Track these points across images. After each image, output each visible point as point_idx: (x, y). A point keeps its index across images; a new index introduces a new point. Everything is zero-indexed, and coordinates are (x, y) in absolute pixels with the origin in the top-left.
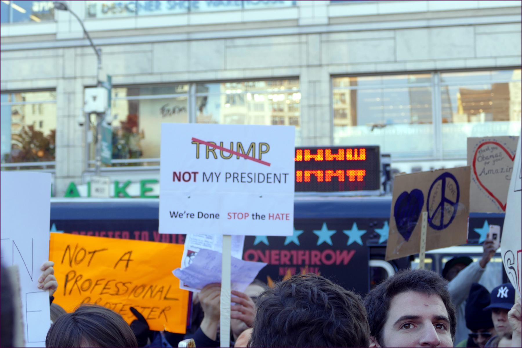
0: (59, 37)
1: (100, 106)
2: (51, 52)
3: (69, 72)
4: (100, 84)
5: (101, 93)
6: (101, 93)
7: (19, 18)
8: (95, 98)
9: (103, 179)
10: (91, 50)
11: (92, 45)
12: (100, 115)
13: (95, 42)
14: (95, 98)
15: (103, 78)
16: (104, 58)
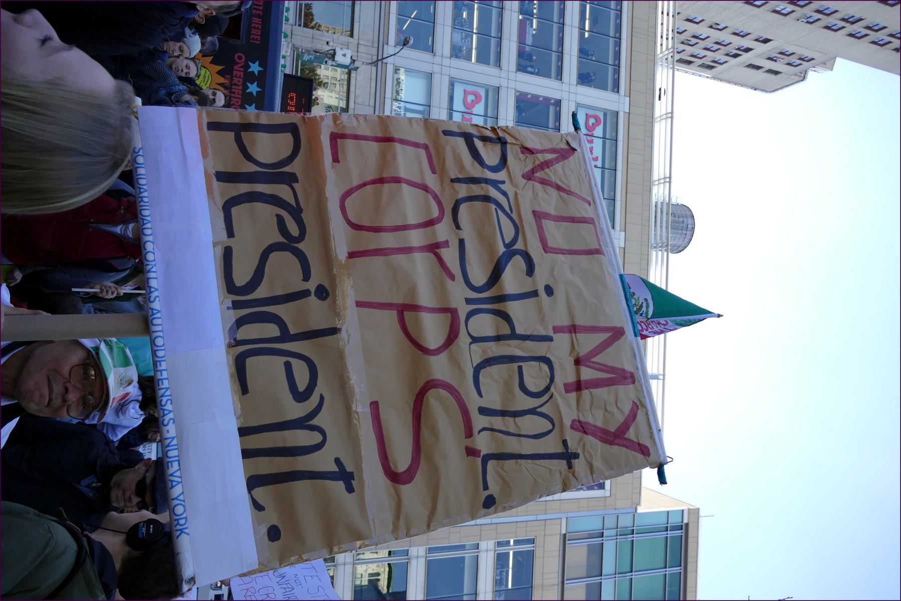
0: (385, 46)
1: (339, 58)
2: (376, 39)
3: (361, 49)
4: (353, 61)
5: (347, 61)
6: (347, 61)
7: (400, 23)
8: (344, 55)
9: (289, 50)
10: (375, 58)
11: (378, 60)
12: (333, 56)
13: (380, 63)
14: (344, 55)
15: (356, 64)
16: (369, 67)
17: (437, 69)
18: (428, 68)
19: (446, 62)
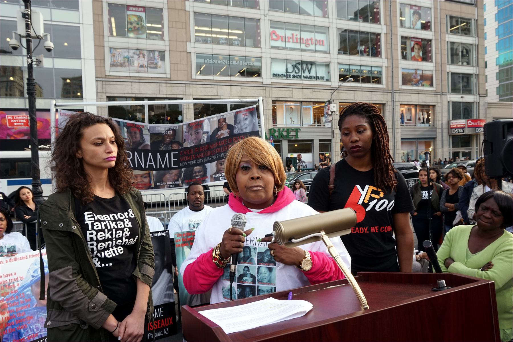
17: (268, 56)
18: (269, 60)
19: (264, 50)
